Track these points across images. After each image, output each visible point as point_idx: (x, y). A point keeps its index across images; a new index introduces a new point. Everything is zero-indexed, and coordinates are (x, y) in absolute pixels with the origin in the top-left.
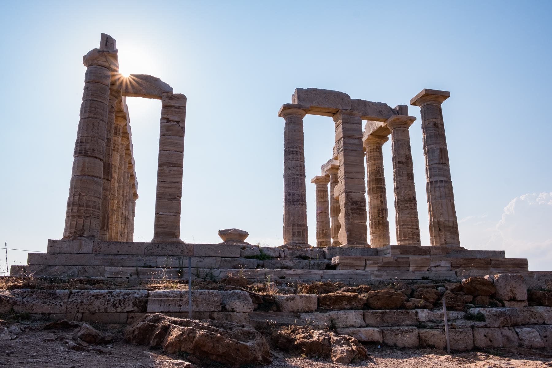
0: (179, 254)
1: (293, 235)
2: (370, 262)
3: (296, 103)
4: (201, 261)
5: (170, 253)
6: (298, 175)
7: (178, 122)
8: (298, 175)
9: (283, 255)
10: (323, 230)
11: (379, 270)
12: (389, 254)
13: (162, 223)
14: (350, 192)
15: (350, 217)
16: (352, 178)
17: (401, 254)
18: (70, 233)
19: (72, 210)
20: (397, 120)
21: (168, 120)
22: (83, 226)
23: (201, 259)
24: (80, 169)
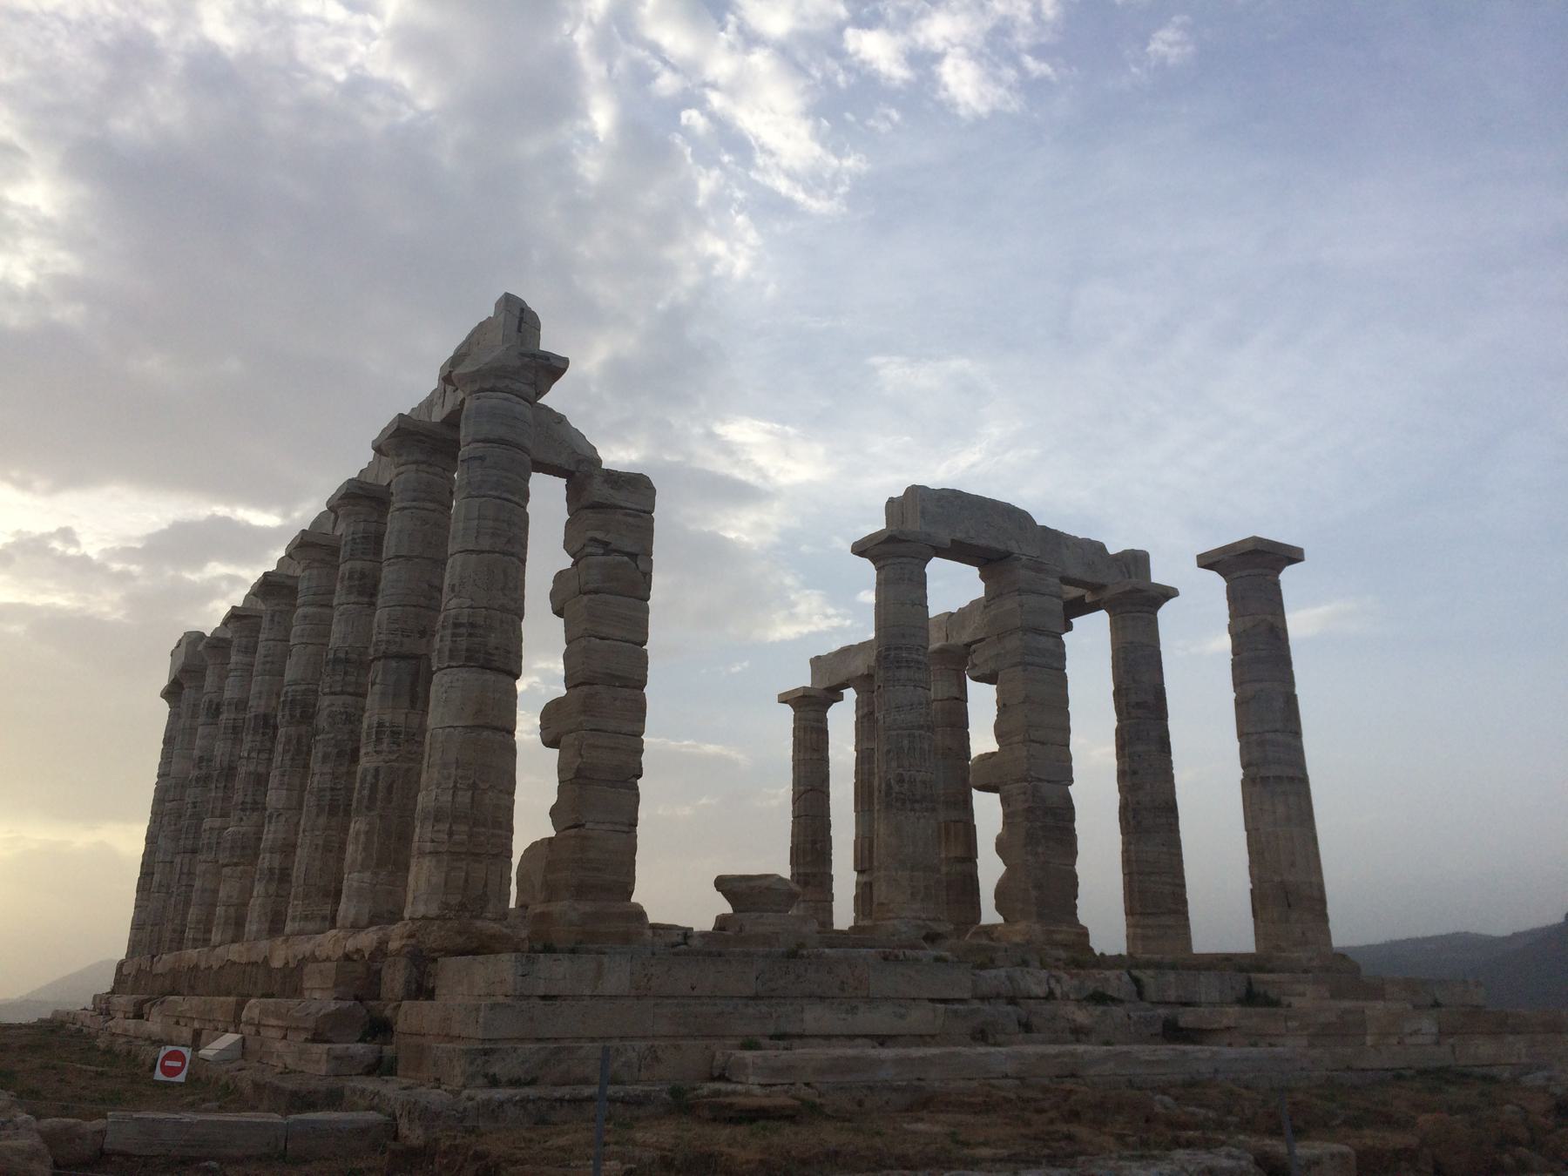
1: (912, 894)
2: (1295, 1024)
3: (914, 525)
4: (902, 1017)
6: (921, 727)
7: (633, 556)
8: (921, 727)
9: (1058, 992)
11: (1311, 1045)
12: (1303, 995)
14: (1040, 780)
15: (1040, 850)
16: (1043, 743)
17: (1333, 997)
18: (446, 906)
19: (451, 834)
20: (1130, 593)
21: (607, 548)
22: (486, 885)
23: (903, 1011)
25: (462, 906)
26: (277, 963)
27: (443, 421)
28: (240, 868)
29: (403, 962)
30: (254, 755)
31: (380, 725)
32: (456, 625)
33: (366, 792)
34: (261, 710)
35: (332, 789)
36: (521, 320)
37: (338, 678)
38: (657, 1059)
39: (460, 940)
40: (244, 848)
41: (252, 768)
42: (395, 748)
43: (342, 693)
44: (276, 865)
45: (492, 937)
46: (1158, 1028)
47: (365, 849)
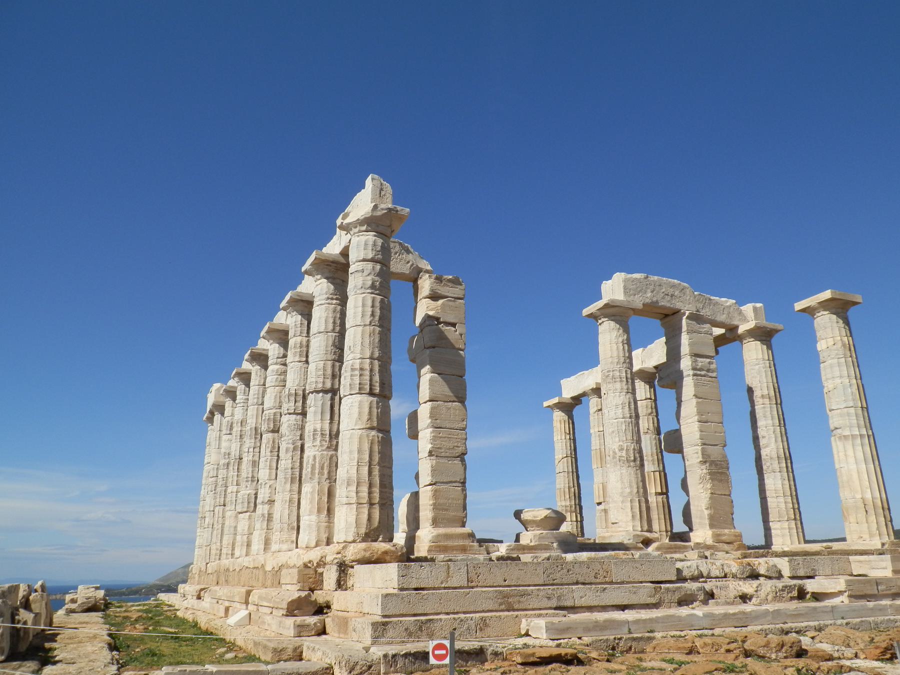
0: (594, 580)
5: (581, 579)
7: (454, 325)
13: (442, 501)
24: (366, 417)
25: (366, 534)
26: (268, 568)
28: (248, 514)
29: (335, 567)
30: (251, 450)
31: (315, 430)
32: (353, 370)
33: (309, 470)
36: (381, 189)
38: (486, 625)
42: (324, 443)
44: (266, 512)
45: (386, 553)
46: (795, 593)
47: (311, 502)
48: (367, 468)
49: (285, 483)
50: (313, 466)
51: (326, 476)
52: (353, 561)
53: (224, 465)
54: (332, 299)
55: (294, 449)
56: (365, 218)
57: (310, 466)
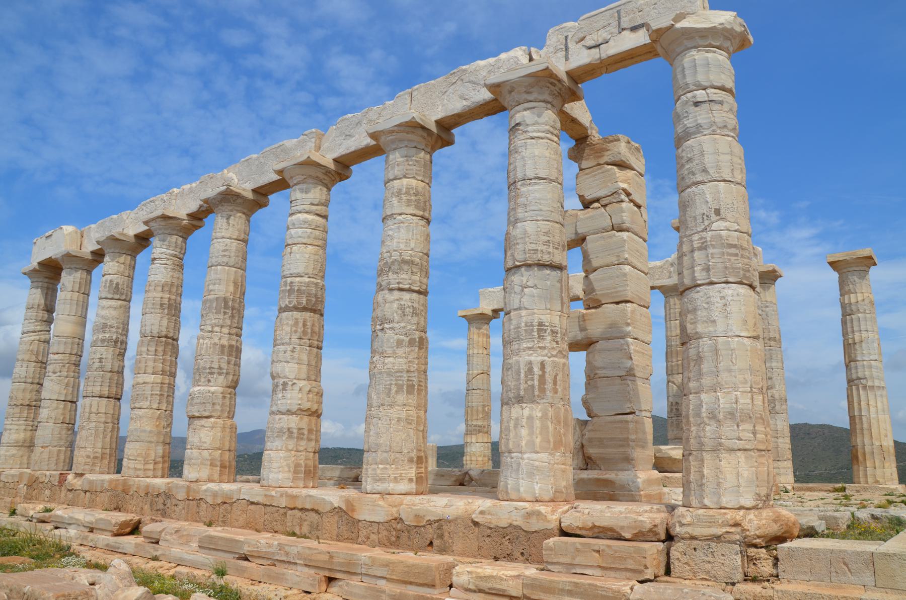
7: (639, 207)
10: (484, 406)
19: (754, 434)
24: (751, 322)
27: (568, 73)
28: (212, 420)
29: (737, 548)
30: (217, 329)
31: (541, 324)
33: (536, 383)
34: (221, 294)
35: (408, 371)
37: (404, 276)
39: (774, 529)
40: (214, 404)
41: (216, 340)
43: (410, 290)
47: (541, 433)
48: (761, 397)
49: (397, 392)
50: (542, 378)
51: (560, 394)
52: (759, 537)
53: (103, 340)
54: (552, 133)
55: (411, 342)
56: (725, 29)
57: (536, 377)
